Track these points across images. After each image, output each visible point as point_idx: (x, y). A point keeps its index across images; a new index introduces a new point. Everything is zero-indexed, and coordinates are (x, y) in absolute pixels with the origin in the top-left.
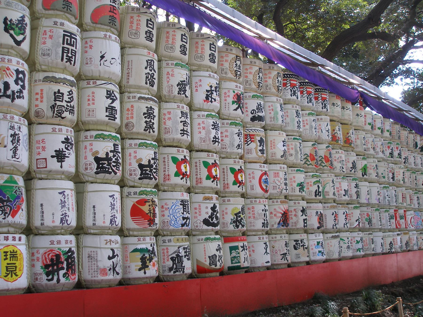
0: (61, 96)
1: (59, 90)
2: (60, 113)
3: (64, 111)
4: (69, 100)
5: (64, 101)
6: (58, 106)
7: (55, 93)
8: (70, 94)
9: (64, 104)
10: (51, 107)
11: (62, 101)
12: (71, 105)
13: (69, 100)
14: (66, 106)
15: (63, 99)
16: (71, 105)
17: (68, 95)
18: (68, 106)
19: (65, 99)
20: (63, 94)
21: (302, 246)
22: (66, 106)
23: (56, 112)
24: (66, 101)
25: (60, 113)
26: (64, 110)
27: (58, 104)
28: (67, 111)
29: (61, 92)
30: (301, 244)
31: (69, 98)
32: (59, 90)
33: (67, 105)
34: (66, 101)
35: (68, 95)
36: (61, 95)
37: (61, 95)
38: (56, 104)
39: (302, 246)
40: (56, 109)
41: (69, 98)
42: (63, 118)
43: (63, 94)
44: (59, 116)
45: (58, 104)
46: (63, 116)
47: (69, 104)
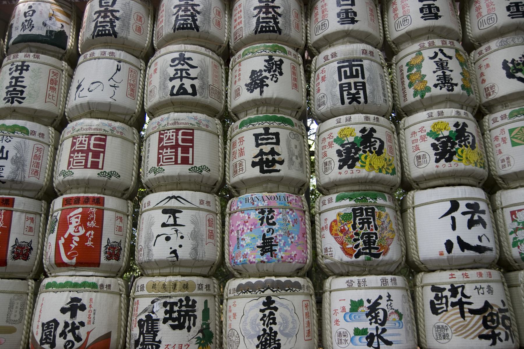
21: (453, 305)
30: (451, 300)
39: (453, 305)
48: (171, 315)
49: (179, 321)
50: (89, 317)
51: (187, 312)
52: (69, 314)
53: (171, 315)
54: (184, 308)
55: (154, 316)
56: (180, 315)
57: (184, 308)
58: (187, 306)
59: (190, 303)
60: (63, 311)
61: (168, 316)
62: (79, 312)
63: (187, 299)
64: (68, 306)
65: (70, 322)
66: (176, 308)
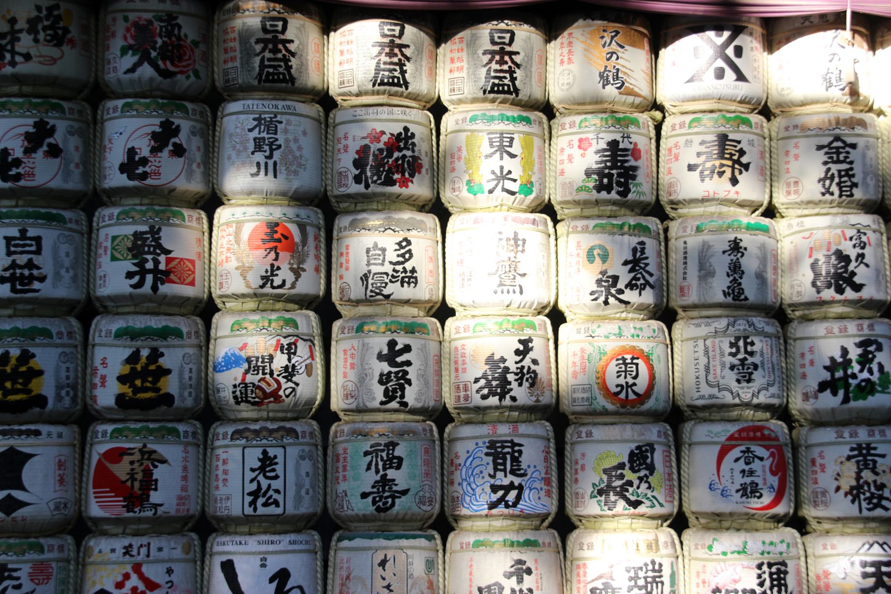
0: (379, 255)
1: (376, 245)
2: (377, 288)
3: (386, 284)
4: (401, 259)
5: (387, 263)
6: (375, 274)
7: (368, 251)
8: (402, 247)
9: (388, 268)
10: (361, 278)
11: (383, 265)
12: (404, 268)
13: (401, 259)
14: (391, 273)
15: (384, 261)
16: (404, 268)
17: (396, 250)
18: (397, 272)
19: (388, 259)
20: (384, 250)
22: (391, 273)
23: (370, 287)
24: (391, 263)
25: (377, 288)
26: (388, 281)
27: (373, 272)
28: (393, 282)
29: (379, 246)
31: (398, 256)
32: (376, 245)
33: (394, 270)
34: (391, 263)
35: (396, 250)
36: (380, 252)
37: (380, 252)
38: (370, 272)
40: (370, 281)
41: (398, 256)
42: (387, 297)
43: (384, 250)
44: (377, 294)
45: (373, 272)
46: (386, 292)
47: (399, 268)
48: (636, 583)
49: (646, 590)
50: (537, 582)
51: (654, 578)
52: (514, 579)
53: (636, 583)
54: (650, 574)
55: (614, 584)
56: (647, 582)
57: (650, 574)
58: (654, 570)
59: (657, 567)
60: (508, 576)
61: (633, 583)
62: (525, 576)
63: (653, 562)
64: (513, 570)
65: (517, 588)
66: (641, 574)
